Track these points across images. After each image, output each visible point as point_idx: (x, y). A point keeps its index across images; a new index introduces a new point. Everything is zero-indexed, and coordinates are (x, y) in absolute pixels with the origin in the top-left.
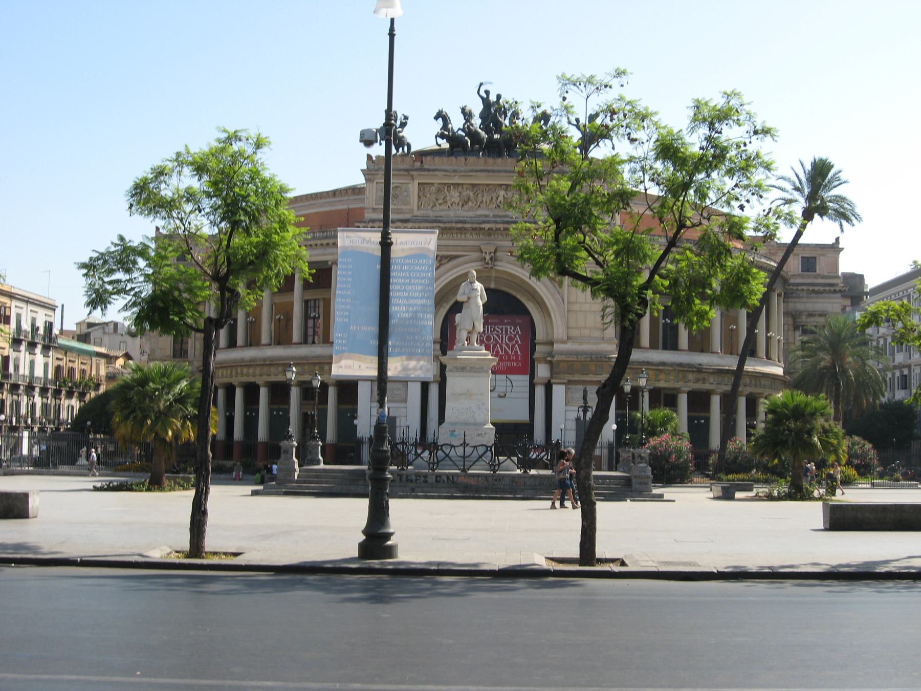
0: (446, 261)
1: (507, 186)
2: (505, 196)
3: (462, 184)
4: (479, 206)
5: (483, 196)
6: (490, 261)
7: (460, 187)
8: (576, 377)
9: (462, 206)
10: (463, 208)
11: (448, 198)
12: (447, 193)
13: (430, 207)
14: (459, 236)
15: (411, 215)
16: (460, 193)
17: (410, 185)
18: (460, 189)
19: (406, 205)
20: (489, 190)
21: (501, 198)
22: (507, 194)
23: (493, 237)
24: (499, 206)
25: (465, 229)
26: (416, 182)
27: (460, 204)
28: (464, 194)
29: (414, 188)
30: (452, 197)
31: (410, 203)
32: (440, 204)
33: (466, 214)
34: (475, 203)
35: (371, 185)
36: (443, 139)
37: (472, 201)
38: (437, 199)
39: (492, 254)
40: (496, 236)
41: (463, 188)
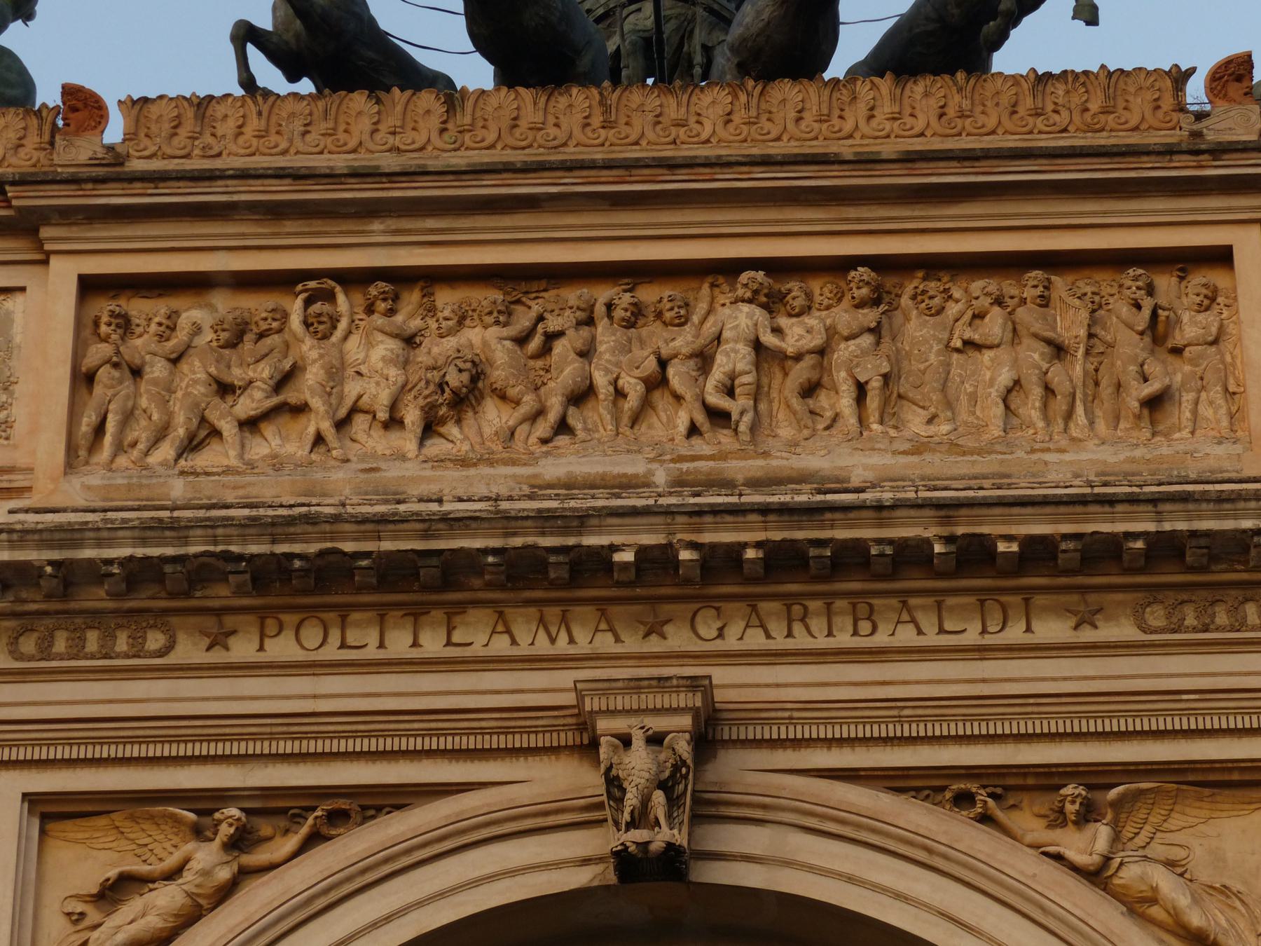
0: (291, 843)
1: (776, 267)
2: (769, 339)
4: (563, 427)
5: (586, 354)
6: (659, 797)
7: (412, 298)
9: (430, 429)
10: (436, 447)
11: (313, 376)
13: (166, 451)
16: (410, 341)
18: (408, 316)
22: (777, 331)
23: (678, 639)
24: (719, 417)
27: (412, 416)
28: (437, 348)
32: (251, 424)
33: (450, 481)
34: (524, 410)
36: (293, 77)
37: (503, 397)
39: (684, 748)
41: (432, 310)
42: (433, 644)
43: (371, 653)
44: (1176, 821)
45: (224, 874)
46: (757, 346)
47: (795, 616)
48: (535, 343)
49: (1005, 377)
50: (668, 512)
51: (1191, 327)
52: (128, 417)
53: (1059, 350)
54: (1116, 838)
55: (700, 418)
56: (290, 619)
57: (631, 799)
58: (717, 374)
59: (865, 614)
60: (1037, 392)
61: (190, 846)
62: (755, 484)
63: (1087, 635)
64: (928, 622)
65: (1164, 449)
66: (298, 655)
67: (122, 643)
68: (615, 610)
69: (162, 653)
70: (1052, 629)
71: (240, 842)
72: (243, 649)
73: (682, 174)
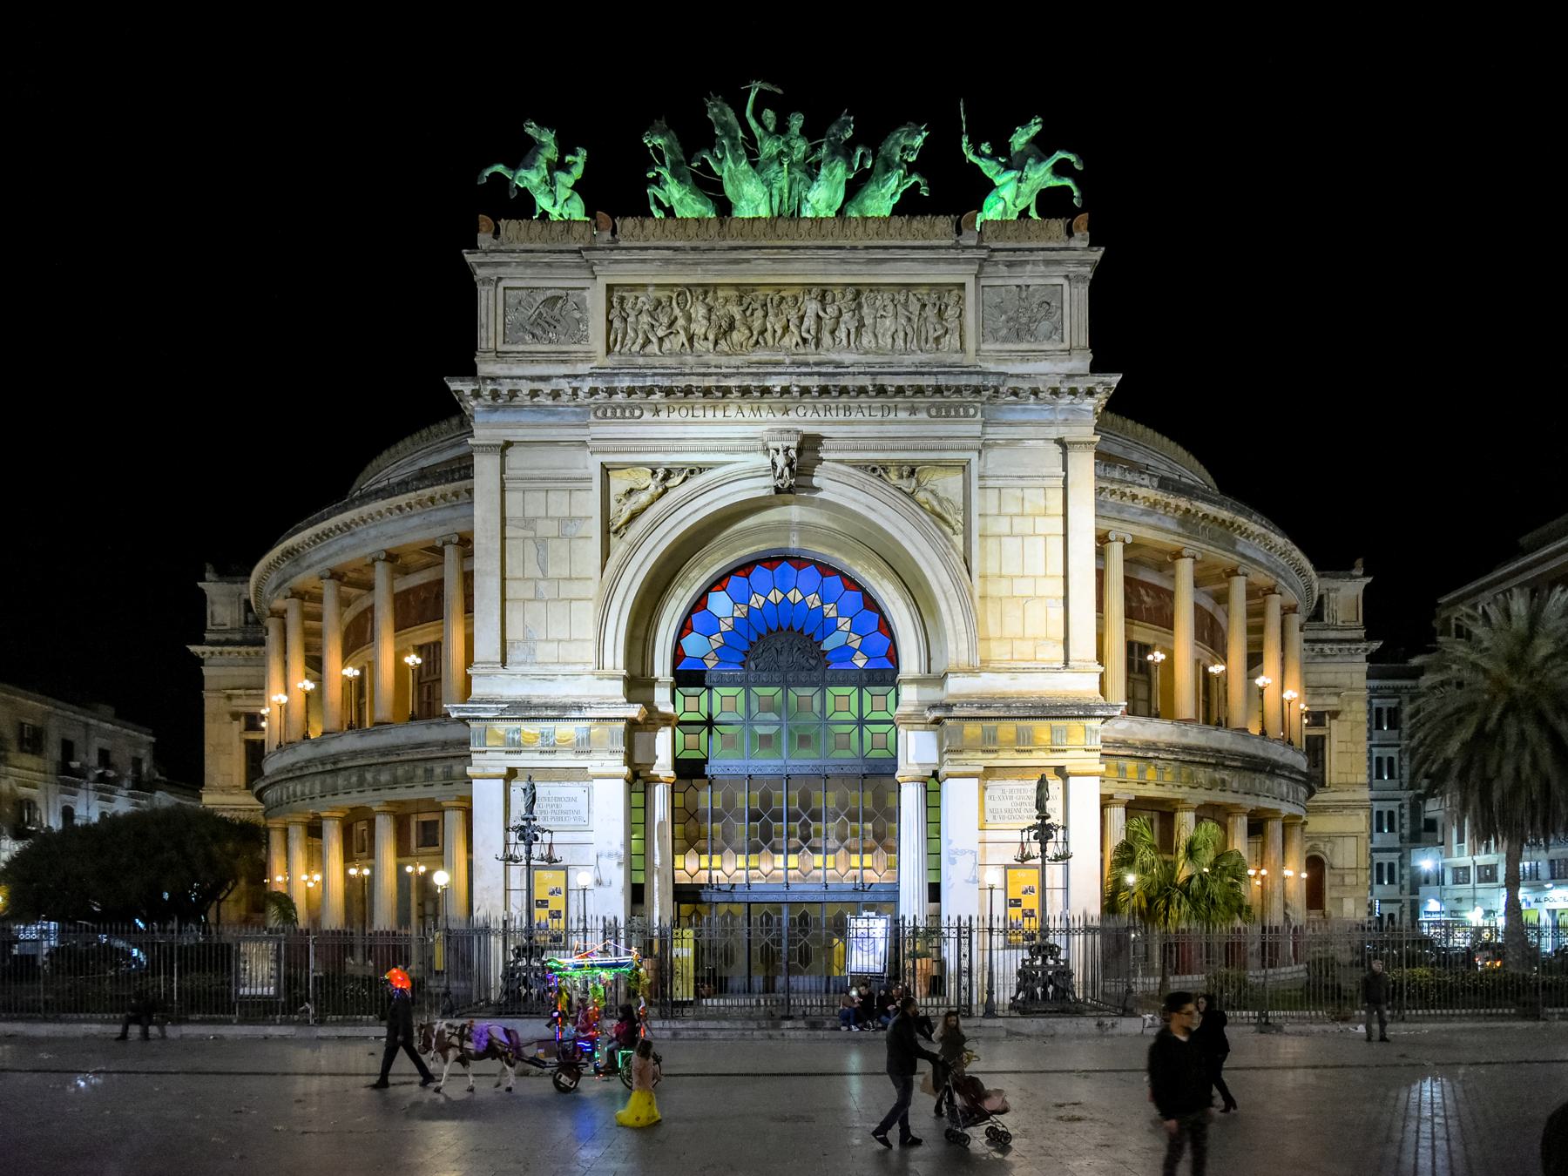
2: (821, 314)
3: (716, 286)
4: (757, 342)
6: (787, 469)
8: (1005, 759)
9: (716, 343)
12: (677, 311)
13: (636, 348)
14: (710, 414)
15: (595, 364)
16: (710, 310)
17: (586, 293)
19: (579, 342)
20: (782, 298)
21: (810, 322)
22: (825, 311)
23: (792, 415)
24: (805, 341)
25: (726, 391)
26: (602, 282)
27: (711, 337)
29: (595, 299)
30: (689, 319)
31: (587, 337)
35: (491, 294)
38: (653, 326)
40: (801, 412)
42: (719, 414)
43: (702, 418)
44: (935, 477)
45: (660, 490)
46: (818, 316)
47: (827, 409)
48: (748, 313)
49: (893, 329)
50: (791, 374)
51: (950, 312)
52: (625, 334)
53: (909, 319)
54: (919, 483)
55: (800, 341)
56: (677, 407)
57: (779, 470)
58: (804, 328)
59: (848, 409)
60: (902, 335)
61: (650, 481)
62: (817, 364)
63: (913, 417)
64: (866, 412)
65: (939, 355)
66: (679, 419)
67: (627, 414)
68: (773, 406)
69: (639, 417)
70: (903, 415)
71: (666, 478)
72: (663, 415)
73: (795, 252)
